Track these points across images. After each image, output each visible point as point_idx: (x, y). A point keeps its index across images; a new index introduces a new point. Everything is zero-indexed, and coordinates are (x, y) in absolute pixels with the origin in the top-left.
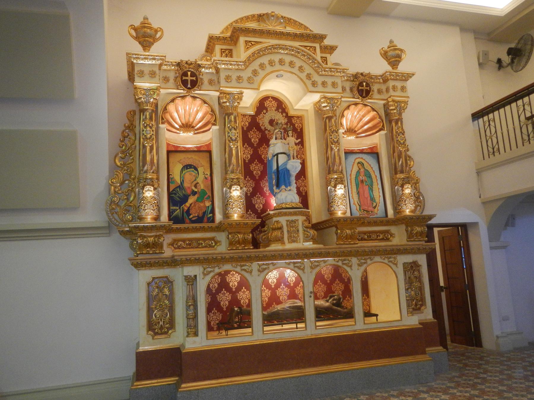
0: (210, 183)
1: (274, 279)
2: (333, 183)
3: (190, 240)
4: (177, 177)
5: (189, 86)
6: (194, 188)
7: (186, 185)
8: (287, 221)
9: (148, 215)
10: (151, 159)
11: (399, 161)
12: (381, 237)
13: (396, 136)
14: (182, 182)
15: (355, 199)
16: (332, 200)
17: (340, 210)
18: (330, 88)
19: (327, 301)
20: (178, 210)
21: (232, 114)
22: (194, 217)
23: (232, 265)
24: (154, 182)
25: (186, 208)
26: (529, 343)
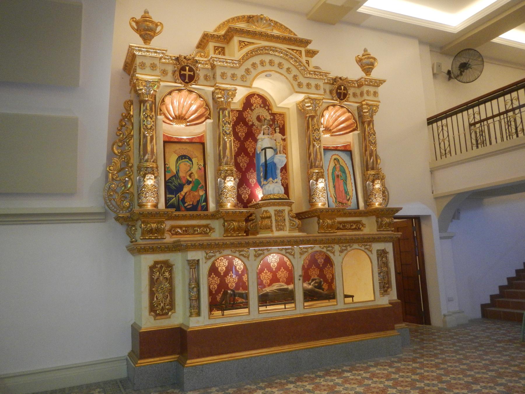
0: (203, 173)
1: (275, 263)
2: (315, 177)
3: (186, 227)
4: (173, 167)
5: (187, 80)
6: (188, 178)
7: (181, 174)
8: (275, 211)
9: (149, 202)
10: (152, 148)
11: (370, 159)
12: (354, 227)
13: (368, 136)
14: (178, 171)
15: (332, 193)
16: (314, 192)
17: (321, 202)
18: (313, 90)
19: (310, 284)
21: (226, 109)
22: (189, 205)
23: (231, 250)
24: (155, 171)
25: (182, 197)
26: (469, 320)
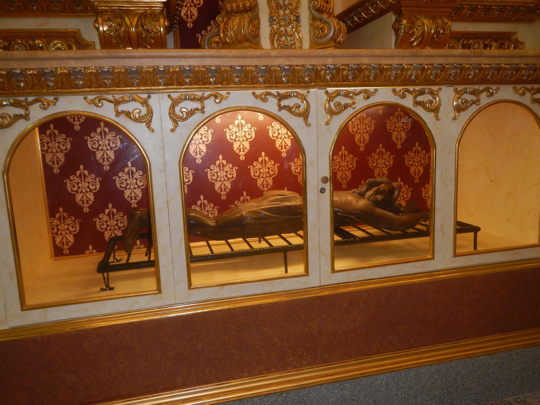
19: (362, 195)
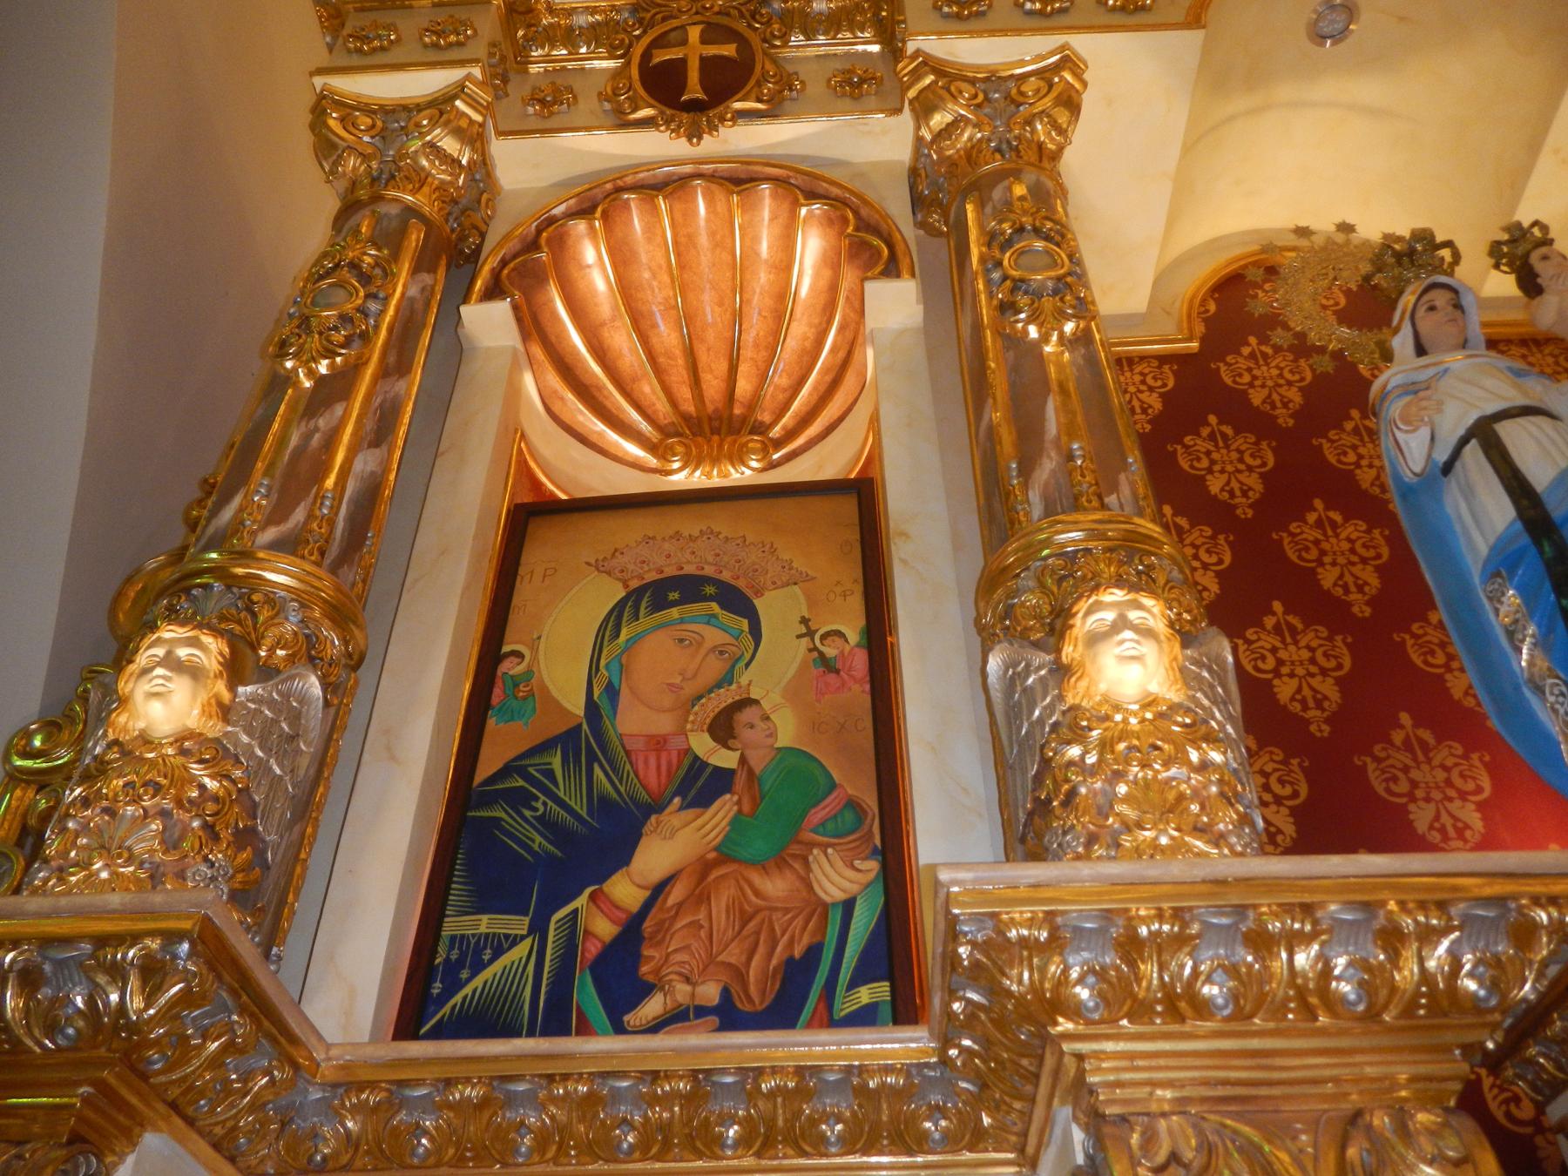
0: (859, 695)
20: (515, 941)
25: (605, 929)
